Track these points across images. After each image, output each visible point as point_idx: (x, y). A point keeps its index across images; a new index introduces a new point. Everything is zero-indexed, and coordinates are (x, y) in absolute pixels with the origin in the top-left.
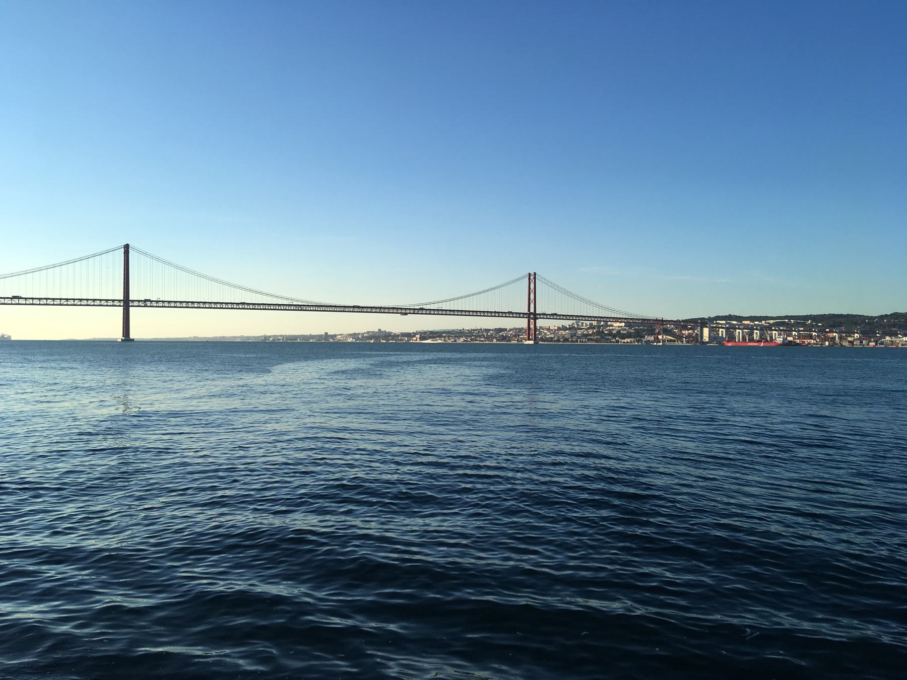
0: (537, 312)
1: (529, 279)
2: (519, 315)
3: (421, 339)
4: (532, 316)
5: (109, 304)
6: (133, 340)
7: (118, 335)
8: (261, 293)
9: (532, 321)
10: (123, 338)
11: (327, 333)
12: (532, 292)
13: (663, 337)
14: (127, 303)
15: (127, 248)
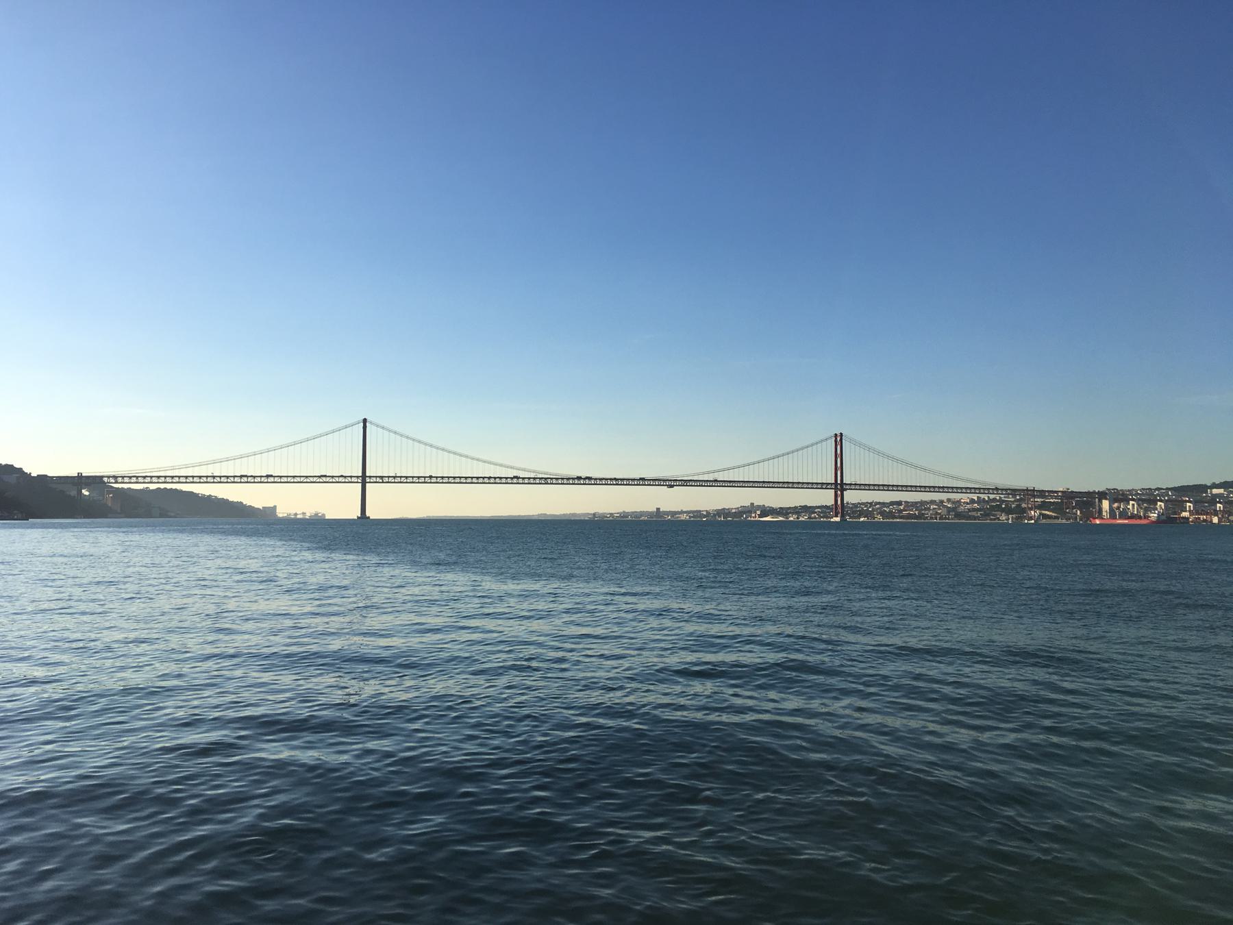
0: (844, 482)
1: (836, 439)
2: (823, 486)
3: (760, 516)
4: (839, 487)
5: (132, 481)
6: (369, 517)
7: (355, 513)
8: (501, 465)
9: (839, 492)
10: (359, 516)
11: (659, 509)
12: (839, 456)
13: (1035, 512)
14: (364, 479)
15: (365, 421)
